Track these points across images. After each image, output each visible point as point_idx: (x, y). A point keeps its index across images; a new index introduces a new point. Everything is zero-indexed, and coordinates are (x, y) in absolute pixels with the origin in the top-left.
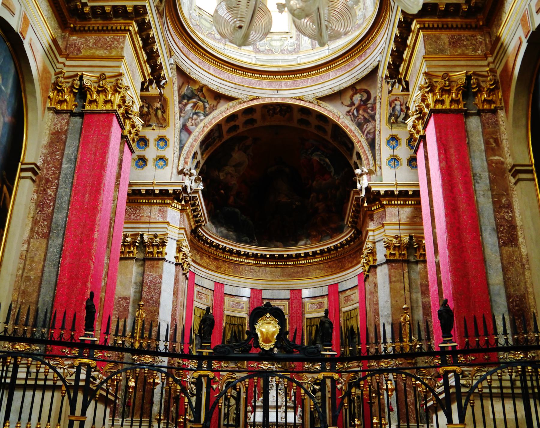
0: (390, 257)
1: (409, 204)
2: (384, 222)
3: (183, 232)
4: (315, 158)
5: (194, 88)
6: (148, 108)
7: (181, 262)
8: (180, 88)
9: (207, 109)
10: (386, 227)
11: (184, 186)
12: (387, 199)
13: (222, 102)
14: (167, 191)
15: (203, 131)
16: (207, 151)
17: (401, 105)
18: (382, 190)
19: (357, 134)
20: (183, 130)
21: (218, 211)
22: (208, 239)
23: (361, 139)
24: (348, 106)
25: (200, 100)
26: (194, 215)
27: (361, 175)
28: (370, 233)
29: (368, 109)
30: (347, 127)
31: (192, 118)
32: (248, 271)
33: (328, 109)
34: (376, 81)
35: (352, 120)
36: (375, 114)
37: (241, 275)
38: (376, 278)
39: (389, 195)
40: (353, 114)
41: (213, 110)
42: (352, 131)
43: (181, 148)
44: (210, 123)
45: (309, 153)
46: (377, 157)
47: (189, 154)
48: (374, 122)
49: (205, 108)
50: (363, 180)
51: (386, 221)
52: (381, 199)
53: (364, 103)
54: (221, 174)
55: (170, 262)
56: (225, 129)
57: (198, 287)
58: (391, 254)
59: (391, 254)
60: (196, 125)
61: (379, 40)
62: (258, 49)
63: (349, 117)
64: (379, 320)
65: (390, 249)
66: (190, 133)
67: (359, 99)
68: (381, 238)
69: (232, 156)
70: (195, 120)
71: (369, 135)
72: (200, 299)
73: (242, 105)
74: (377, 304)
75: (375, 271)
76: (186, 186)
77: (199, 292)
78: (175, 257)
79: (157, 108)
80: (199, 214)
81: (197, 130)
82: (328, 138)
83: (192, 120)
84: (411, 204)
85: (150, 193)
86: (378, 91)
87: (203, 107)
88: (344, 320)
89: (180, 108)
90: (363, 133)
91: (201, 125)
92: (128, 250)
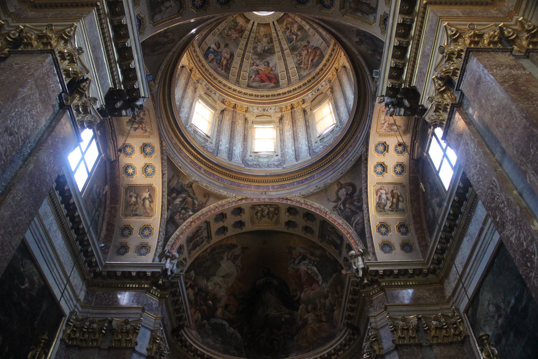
0: (399, 341)
1: (410, 285)
2: (387, 304)
3: (160, 321)
4: (303, 267)
5: (184, 184)
6: (136, 198)
7: (153, 355)
8: (169, 181)
9: (196, 205)
10: (389, 309)
11: (164, 268)
13: (211, 199)
14: (145, 272)
15: (190, 225)
16: (195, 251)
17: (386, 194)
18: (381, 270)
19: (346, 227)
21: (205, 321)
22: (192, 345)
24: (334, 202)
25: (190, 196)
26: (176, 310)
27: (356, 256)
28: (372, 320)
29: (355, 201)
30: (335, 221)
31: (180, 212)
33: (315, 206)
34: (361, 172)
35: (339, 215)
36: (362, 205)
39: (388, 273)
40: (340, 209)
43: (166, 240)
44: (199, 218)
45: (296, 262)
46: (369, 245)
47: (174, 246)
48: (361, 213)
49: (194, 204)
50: (358, 261)
51: (388, 303)
52: (380, 280)
53: (350, 196)
54: (209, 284)
56: (215, 227)
58: (400, 338)
60: (185, 220)
61: (359, 136)
62: (247, 163)
63: (335, 212)
65: (397, 332)
66: (177, 226)
67: (345, 193)
68: (385, 323)
69: (220, 265)
73: (230, 204)
76: (166, 270)
78: (147, 349)
79: (145, 198)
80: (180, 308)
81: (185, 223)
82: (315, 239)
83: (180, 214)
84: (412, 285)
85: (127, 276)
86: (363, 182)
87: (192, 203)
89: (168, 200)
90: (352, 226)
91: (190, 219)
92: (93, 338)
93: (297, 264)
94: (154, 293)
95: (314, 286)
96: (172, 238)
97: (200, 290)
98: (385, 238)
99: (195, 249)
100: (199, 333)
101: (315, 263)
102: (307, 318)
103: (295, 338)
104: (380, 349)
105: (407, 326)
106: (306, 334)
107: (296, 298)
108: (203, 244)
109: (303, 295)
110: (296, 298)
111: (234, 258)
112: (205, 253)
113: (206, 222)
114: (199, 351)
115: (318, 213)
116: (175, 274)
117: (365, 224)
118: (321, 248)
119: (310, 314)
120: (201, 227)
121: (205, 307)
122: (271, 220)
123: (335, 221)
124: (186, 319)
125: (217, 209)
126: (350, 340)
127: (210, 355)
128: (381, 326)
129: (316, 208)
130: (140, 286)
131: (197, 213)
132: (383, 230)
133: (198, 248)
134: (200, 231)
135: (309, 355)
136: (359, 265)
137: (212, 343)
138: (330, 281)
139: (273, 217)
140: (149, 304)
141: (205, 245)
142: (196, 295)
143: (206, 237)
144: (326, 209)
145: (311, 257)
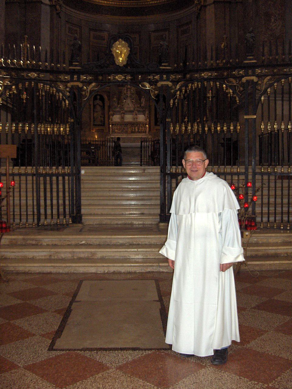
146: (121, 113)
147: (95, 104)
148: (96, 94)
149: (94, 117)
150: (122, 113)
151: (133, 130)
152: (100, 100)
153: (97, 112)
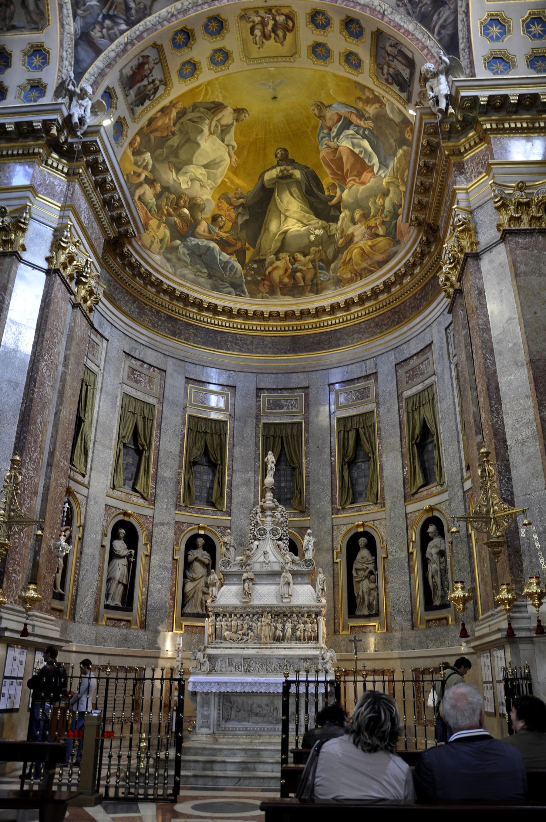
0: (510, 226)
2: (491, 161)
12: (493, 118)
14: (30, 123)
15: (124, 50)
16: (141, 108)
18: (483, 95)
19: (420, 37)
20: (81, 42)
21: (178, 242)
22: (150, 273)
23: (429, 43)
27: (435, 75)
30: (401, 27)
32: (231, 342)
35: (409, 14)
37: (218, 348)
38: (481, 278)
41: (145, 16)
42: (409, 32)
44: (140, 37)
45: (333, 135)
50: (439, 83)
54: (182, 179)
55: (35, 267)
57: (133, 361)
59: (511, 219)
60: (112, 40)
63: (402, 9)
64: (494, 363)
66: (98, 51)
69: (199, 145)
70: (109, 29)
71: (443, 32)
72: (136, 381)
73: (199, 8)
74: (486, 329)
75: (478, 264)
77: (134, 370)
81: (113, 46)
88: (408, 413)
90: (433, 33)
91: (123, 39)
93: (334, 138)
94: (55, 165)
95: (366, 176)
96: (90, 73)
97: (166, 189)
98: (497, 46)
99: (142, 104)
100: (168, 260)
101: (367, 133)
102: (352, 236)
103: (333, 266)
104: (472, 244)
105: (527, 198)
106: (351, 258)
107: (334, 201)
108: (158, 95)
109: (345, 195)
110: (334, 201)
111: (222, 131)
112: (167, 121)
113: (155, 45)
114: (166, 284)
115: (368, 14)
116: (89, 127)
117: (459, 22)
118: (377, 100)
119: (357, 226)
120: (148, 56)
121: (177, 220)
122: (282, 43)
123: (400, 26)
124: (129, 222)
125: (173, 19)
126: (423, 255)
127: (185, 291)
128: (477, 205)
129: (364, 5)
130: (25, 152)
131: (136, 27)
132: (495, 30)
133: (147, 103)
134: (146, 67)
135: (353, 288)
136: (439, 91)
137: (192, 276)
138: (393, 163)
139: (285, 37)
140: (48, 185)
141: (161, 96)
142: (158, 196)
143: (161, 81)
144: (382, 4)
145: (359, 121)
146: (243, 578)
147: (190, 558)
148: (195, 532)
149: (184, 595)
150: (244, 580)
151: (279, 633)
152: (204, 550)
153: (193, 580)
